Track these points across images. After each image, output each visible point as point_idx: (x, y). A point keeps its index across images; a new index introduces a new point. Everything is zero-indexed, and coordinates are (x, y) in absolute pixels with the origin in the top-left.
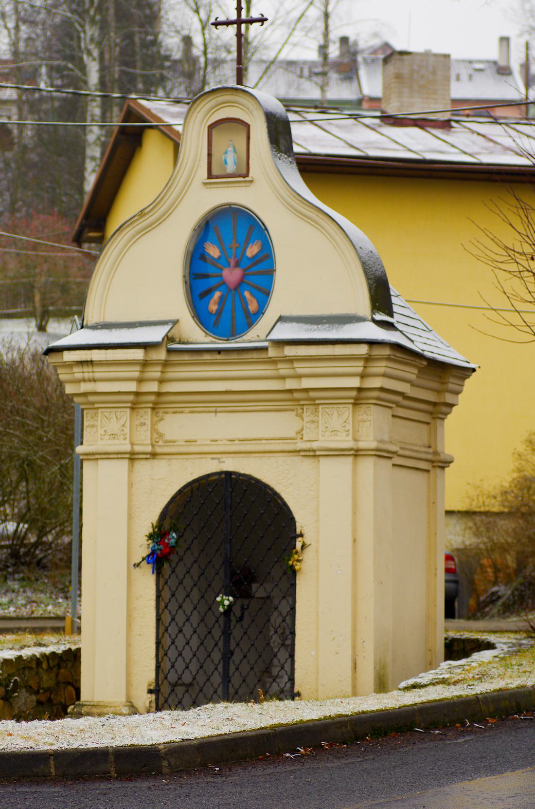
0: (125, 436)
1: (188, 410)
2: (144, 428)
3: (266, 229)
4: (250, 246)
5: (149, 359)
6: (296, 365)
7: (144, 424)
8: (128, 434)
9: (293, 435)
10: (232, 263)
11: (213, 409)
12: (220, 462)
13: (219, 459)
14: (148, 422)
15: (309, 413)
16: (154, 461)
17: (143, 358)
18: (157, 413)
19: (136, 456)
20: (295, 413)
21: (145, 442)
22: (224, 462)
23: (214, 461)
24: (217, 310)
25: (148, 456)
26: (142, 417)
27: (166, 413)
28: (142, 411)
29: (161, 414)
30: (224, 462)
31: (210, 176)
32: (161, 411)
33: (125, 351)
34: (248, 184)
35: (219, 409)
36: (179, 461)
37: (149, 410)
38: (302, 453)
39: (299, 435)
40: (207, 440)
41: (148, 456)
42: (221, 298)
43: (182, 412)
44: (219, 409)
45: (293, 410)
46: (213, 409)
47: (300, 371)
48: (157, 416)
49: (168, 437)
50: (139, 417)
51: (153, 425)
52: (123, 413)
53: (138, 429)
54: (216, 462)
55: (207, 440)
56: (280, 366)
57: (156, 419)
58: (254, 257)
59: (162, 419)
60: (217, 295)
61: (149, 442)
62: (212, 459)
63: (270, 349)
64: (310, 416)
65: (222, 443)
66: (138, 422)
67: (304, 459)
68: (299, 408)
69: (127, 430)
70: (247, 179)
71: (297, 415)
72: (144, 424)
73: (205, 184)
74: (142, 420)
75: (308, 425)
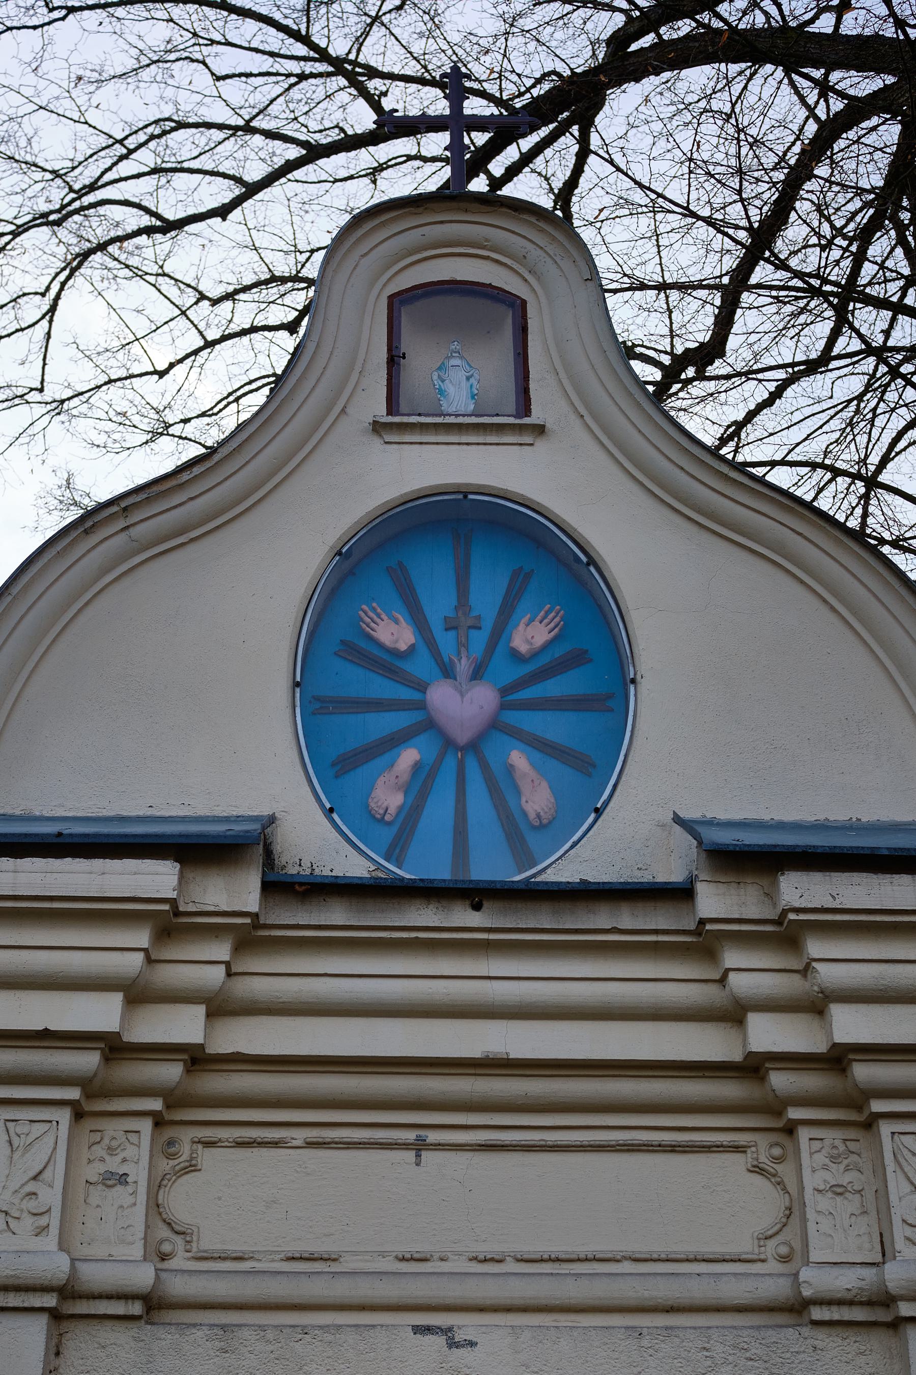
0: (43, 1221)
1: (300, 1135)
2: (120, 1194)
3: (591, 561)
4: (525, 620)
5: (191, 908)
6: (815, 948)
7: (123, 1179)
8: (56, 1213)
9: (745, 1245)
10: (463, 667)
11: (410, 1136)
12: (453, 1344)
13: (447, 1331)
14: (139, 1174)
15: (821, 1158)
16: (160, 1332)
17: (174, 895)
18: (171, 1143)
19: (82, 1307)
20: (736, 1163)
21: (119, 1252)
22: (472, 1344)
23: (430, 1339)
24: (400, 809)
25: (136, 1308)
26: (111, 1151)
27: (209, 1144)
28: (114, 1128)
29: (185, 1150)
30: (472, 1344)
31: (392, 406)
32: (187, 1136)
33: (98, 864)
34: (527, 439)
35: (433, 1137)
36: (270, 1335)
37: (146, 1126)
38: (817, 1313)
39: (771, 1243)
40: (383, 1254)
41: (136, 1308)
42: (417, 767)
43: (275, 1144)
44: (433, 1137)
45: (738, 1149)
46: (410, 1136)
47: (829, 975)
48: (170, 1156)
49: (208, 1242)
50: (99, 1151)
51: (156, 1186)
52: (44, 1127)
53: (94, 1200)
54: (440, 1341)
55: (383, 1254)
56: (732, 958)
57: (165, 1165)
58: (536, 654)
59: (191, 1168)
60: (408, 757)
61: (137, 1251)
62: (418, 1330)
63: (701, 889)
64: (825, 1168)
65: (445, 1267)
66: (93, 1172)
67: (822, 1337)
68: (762, 1140)
69: (51, 1196)
70: (526, 420)
71: (758, 1170)
72: (123, 1179)
73: (378, 427)
74: (113, 1165)
75: (825, 1202)
